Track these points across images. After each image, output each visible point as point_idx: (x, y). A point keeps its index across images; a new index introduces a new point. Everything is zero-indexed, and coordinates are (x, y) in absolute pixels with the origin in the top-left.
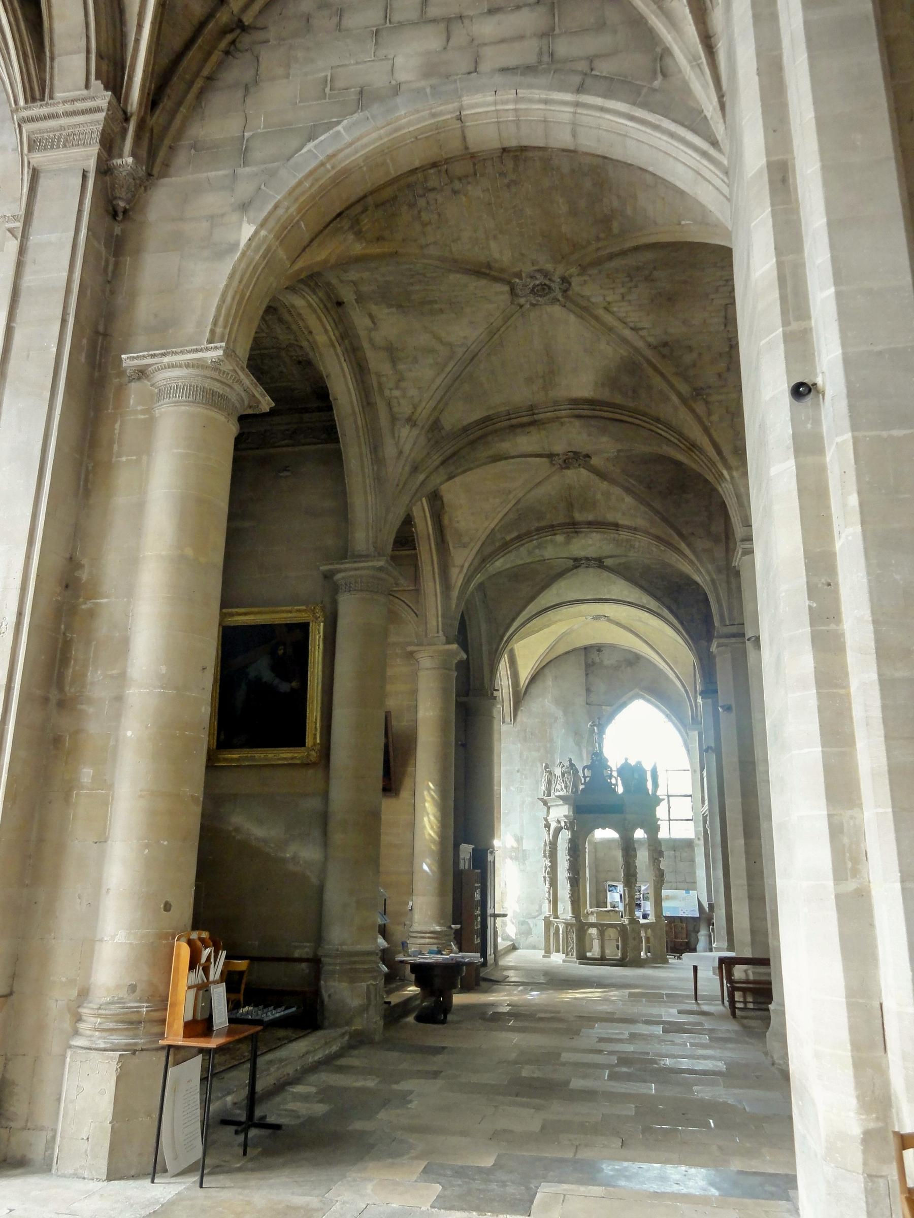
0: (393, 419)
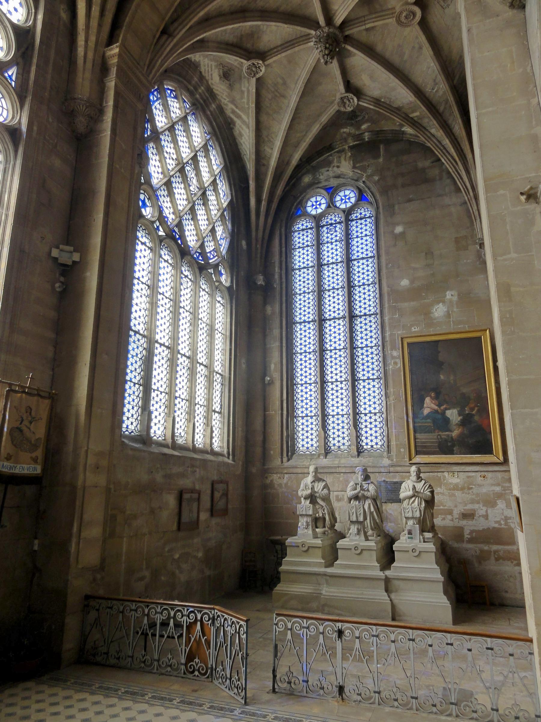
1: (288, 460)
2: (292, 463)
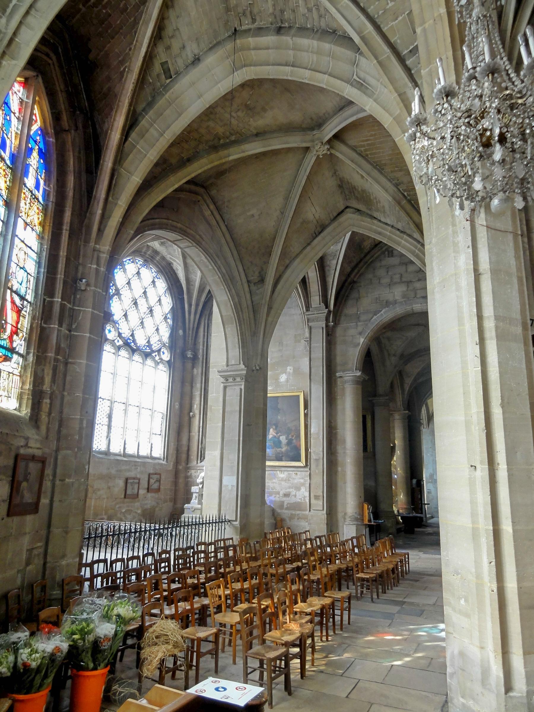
0: (389, 355)
1: (201, 462)
2: (203, 463)
